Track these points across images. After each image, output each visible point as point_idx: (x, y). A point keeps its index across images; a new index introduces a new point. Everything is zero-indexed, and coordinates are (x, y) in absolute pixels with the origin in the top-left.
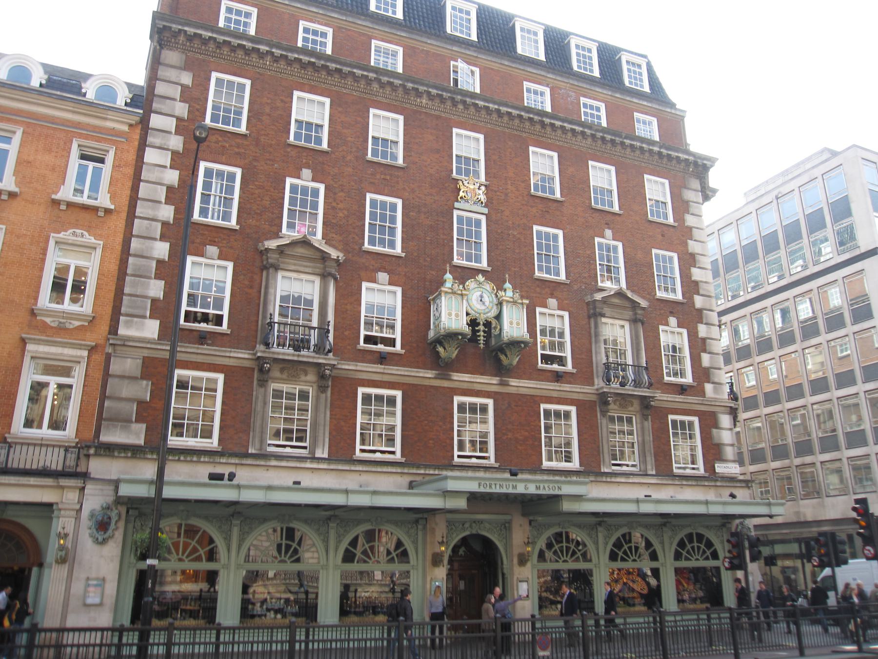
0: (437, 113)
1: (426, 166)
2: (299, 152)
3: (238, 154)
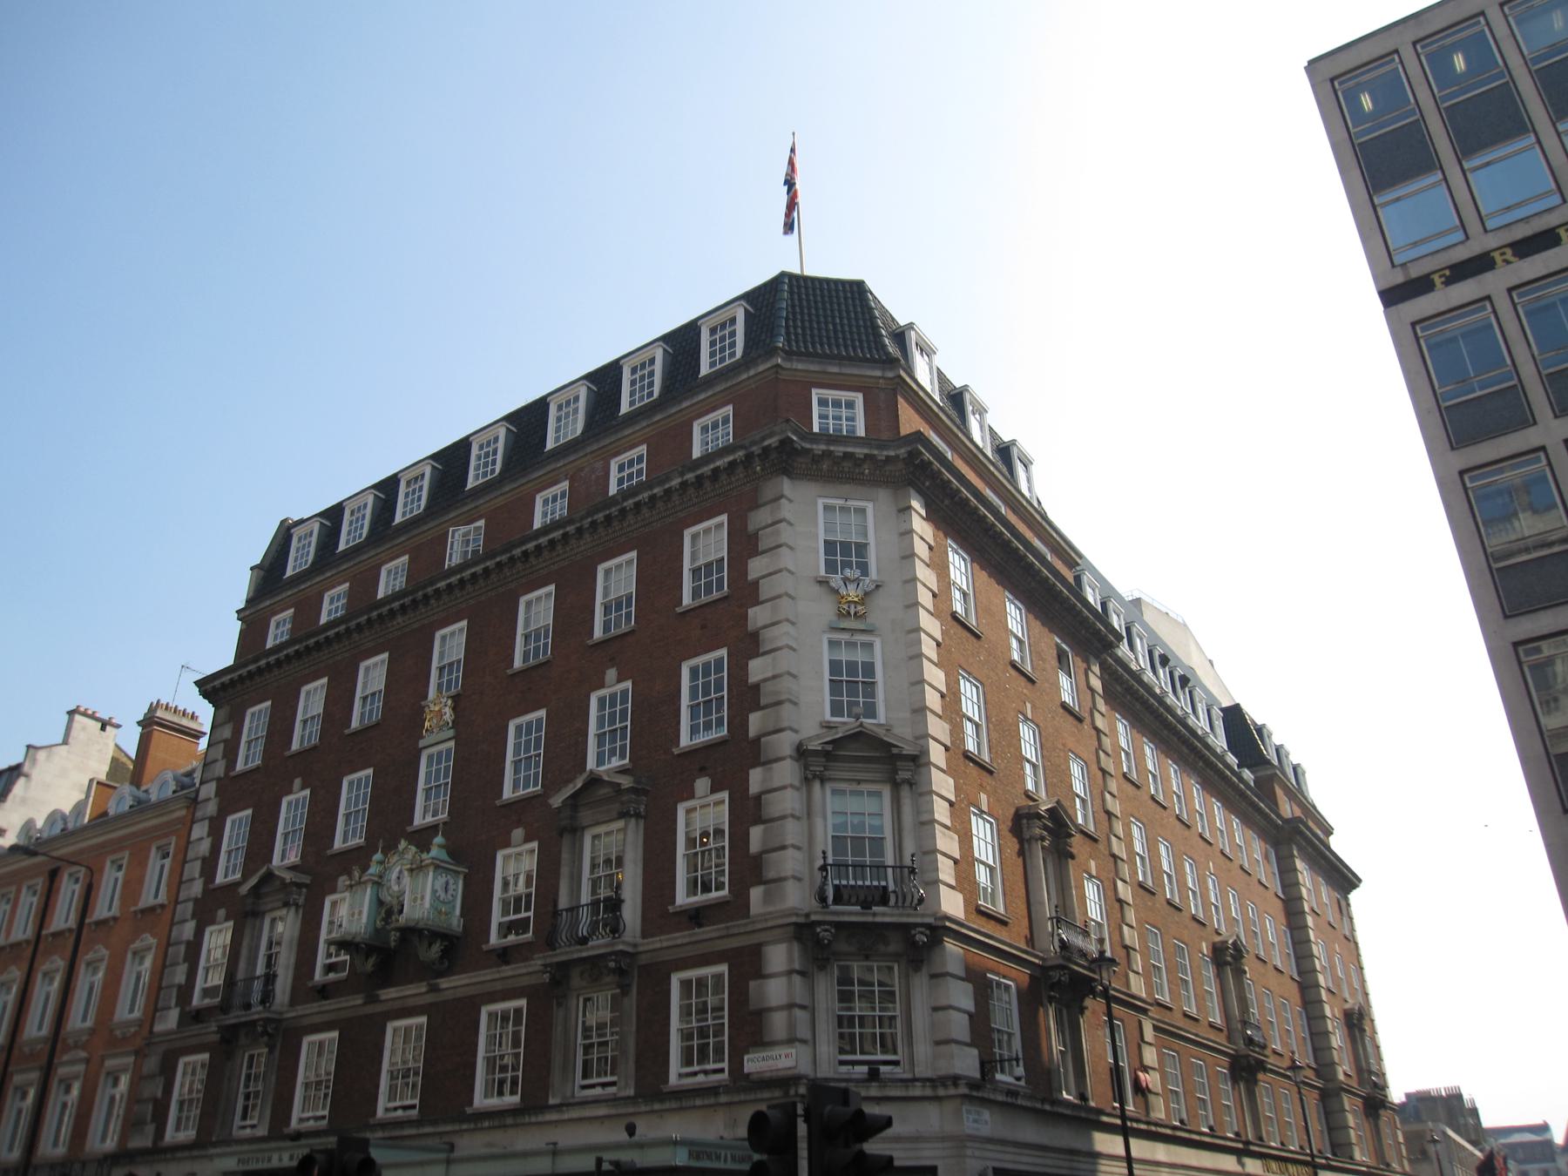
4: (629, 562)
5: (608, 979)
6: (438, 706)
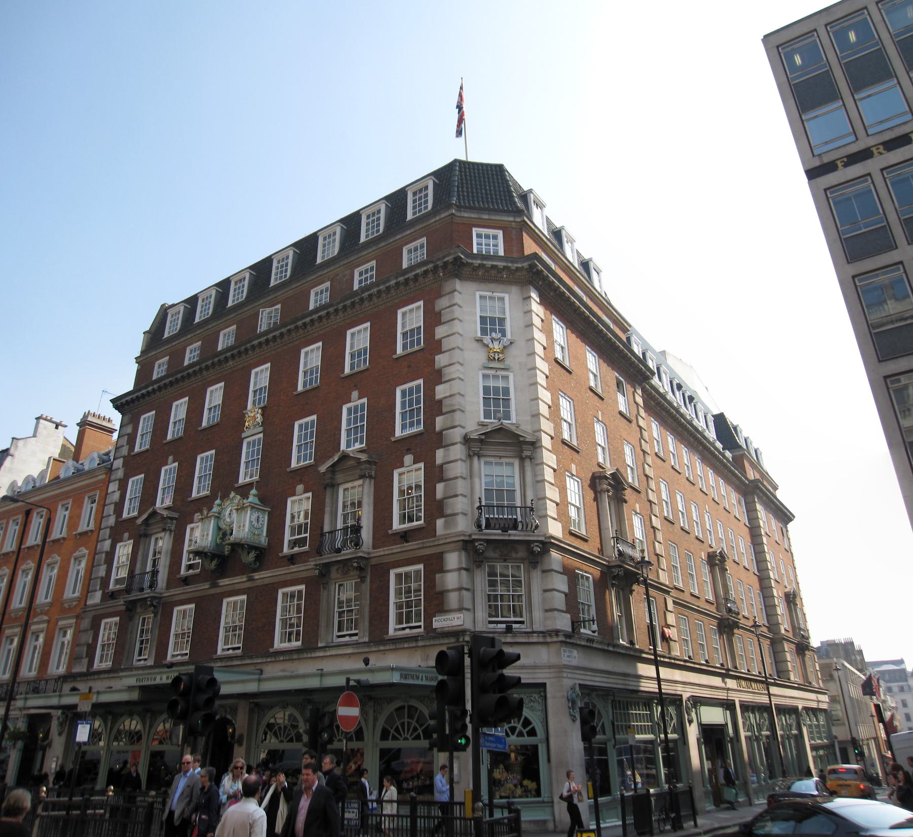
0: (241, 366)
4: (366, 329)
5: (352, 573)
6: (253, 413)
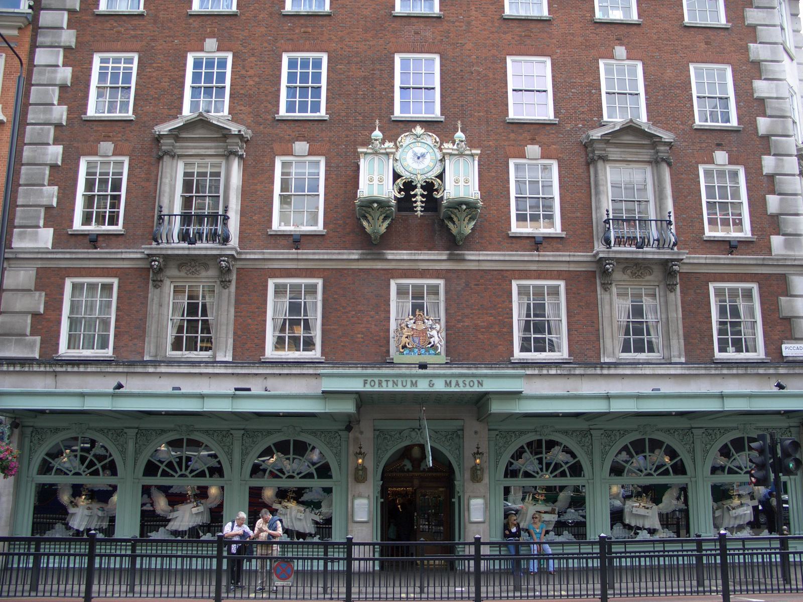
1: (359, 8)
2: (203, 21)
3: (134, 37)
